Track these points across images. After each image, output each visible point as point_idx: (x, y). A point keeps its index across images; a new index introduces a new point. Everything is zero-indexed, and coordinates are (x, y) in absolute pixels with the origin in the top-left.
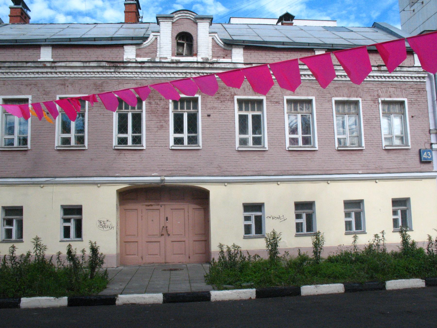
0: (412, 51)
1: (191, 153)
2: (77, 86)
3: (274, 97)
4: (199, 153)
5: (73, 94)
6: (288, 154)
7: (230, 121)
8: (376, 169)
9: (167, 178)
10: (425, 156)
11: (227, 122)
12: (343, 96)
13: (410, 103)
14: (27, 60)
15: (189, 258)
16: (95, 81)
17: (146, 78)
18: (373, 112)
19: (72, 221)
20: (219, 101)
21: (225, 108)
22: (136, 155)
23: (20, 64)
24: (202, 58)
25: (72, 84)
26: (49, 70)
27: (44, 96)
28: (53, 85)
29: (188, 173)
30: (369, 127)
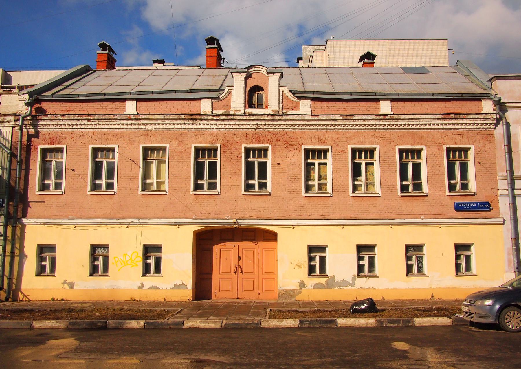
0: (480, 98)
1: (260, 198)
2: (158, 137)
3: (339, 147)
5: (156, 143)
12: (408, 144)
13: (476, 149)
14: (114, 113)
15: (259, 294)
16: (176, 132)
17: (221, 130)
19: (153, 258)
20: (287, 151)
22: (211, 200)
23: (108, 117)
24: (272, 111)
25: (155, 135)
26: (133, 122)
27: (130, 146)
28: (137, 135)
29: (258, 217)
30: (432, 173)
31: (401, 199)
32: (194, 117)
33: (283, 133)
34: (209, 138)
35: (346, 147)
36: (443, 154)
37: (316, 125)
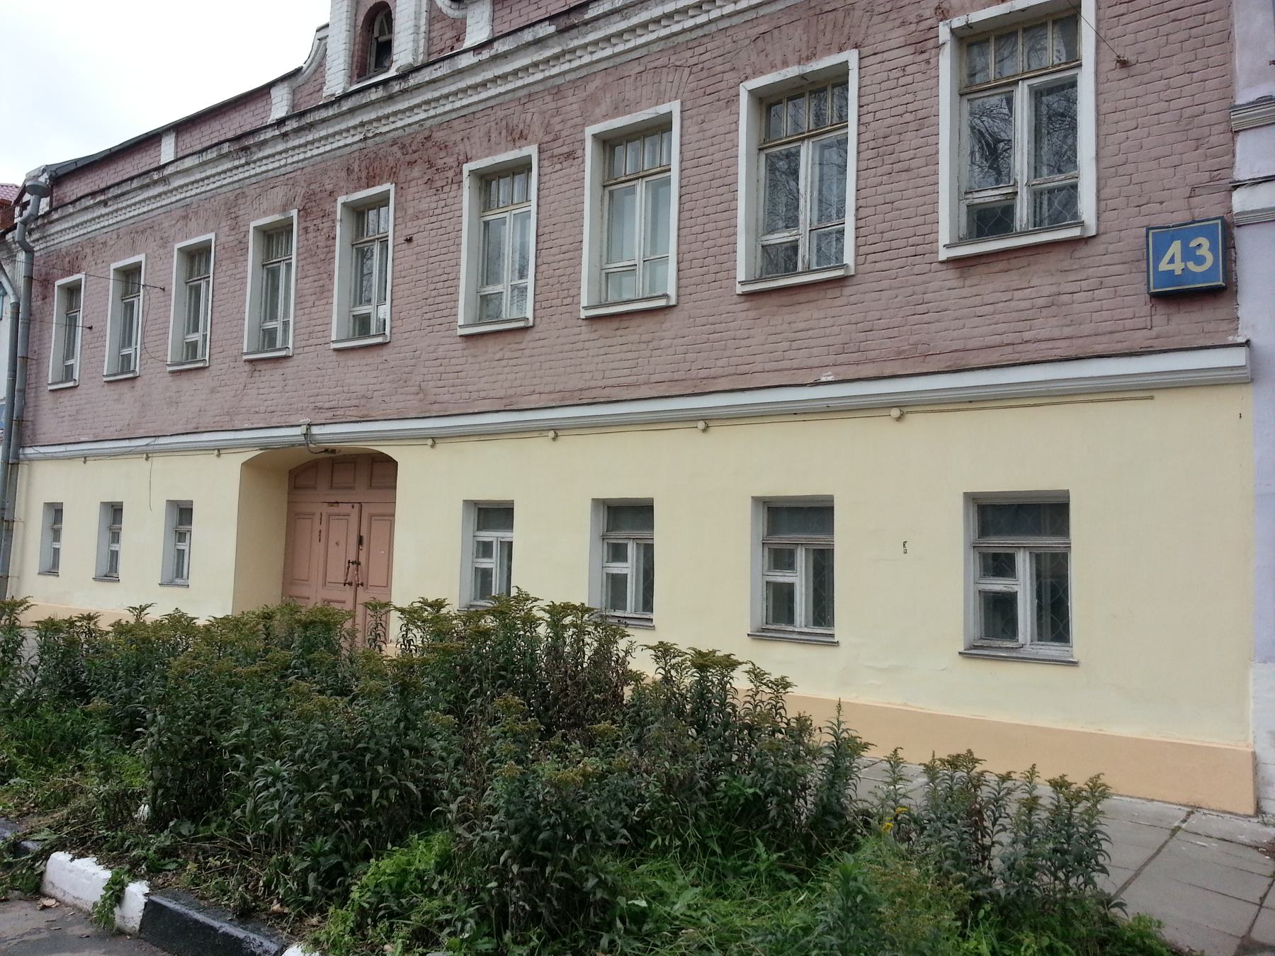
3: (560, 142)
4: (385, 352)
5: (197, 235)
6: (585, 332)
7: (452, 249)
8: (900, 355)
9: (315, 430)
10: (1172, 261)
11: (443, 251)
12: (785, 64)
17: (300, 165)
18: (909, 98)
21: (445, 210)
27: (161, 251)
29: (360, 414)
30: (887, 168)
31: (746, 305)
32: (246, 143)
33: (420, 137)
34: (278, 195)
35: (579, 137)
36: (937, 67)
37: (494, 80)
